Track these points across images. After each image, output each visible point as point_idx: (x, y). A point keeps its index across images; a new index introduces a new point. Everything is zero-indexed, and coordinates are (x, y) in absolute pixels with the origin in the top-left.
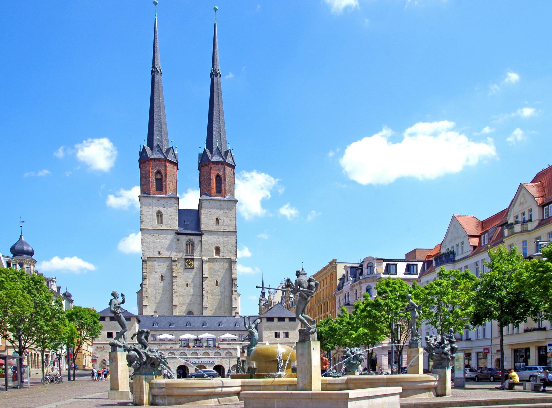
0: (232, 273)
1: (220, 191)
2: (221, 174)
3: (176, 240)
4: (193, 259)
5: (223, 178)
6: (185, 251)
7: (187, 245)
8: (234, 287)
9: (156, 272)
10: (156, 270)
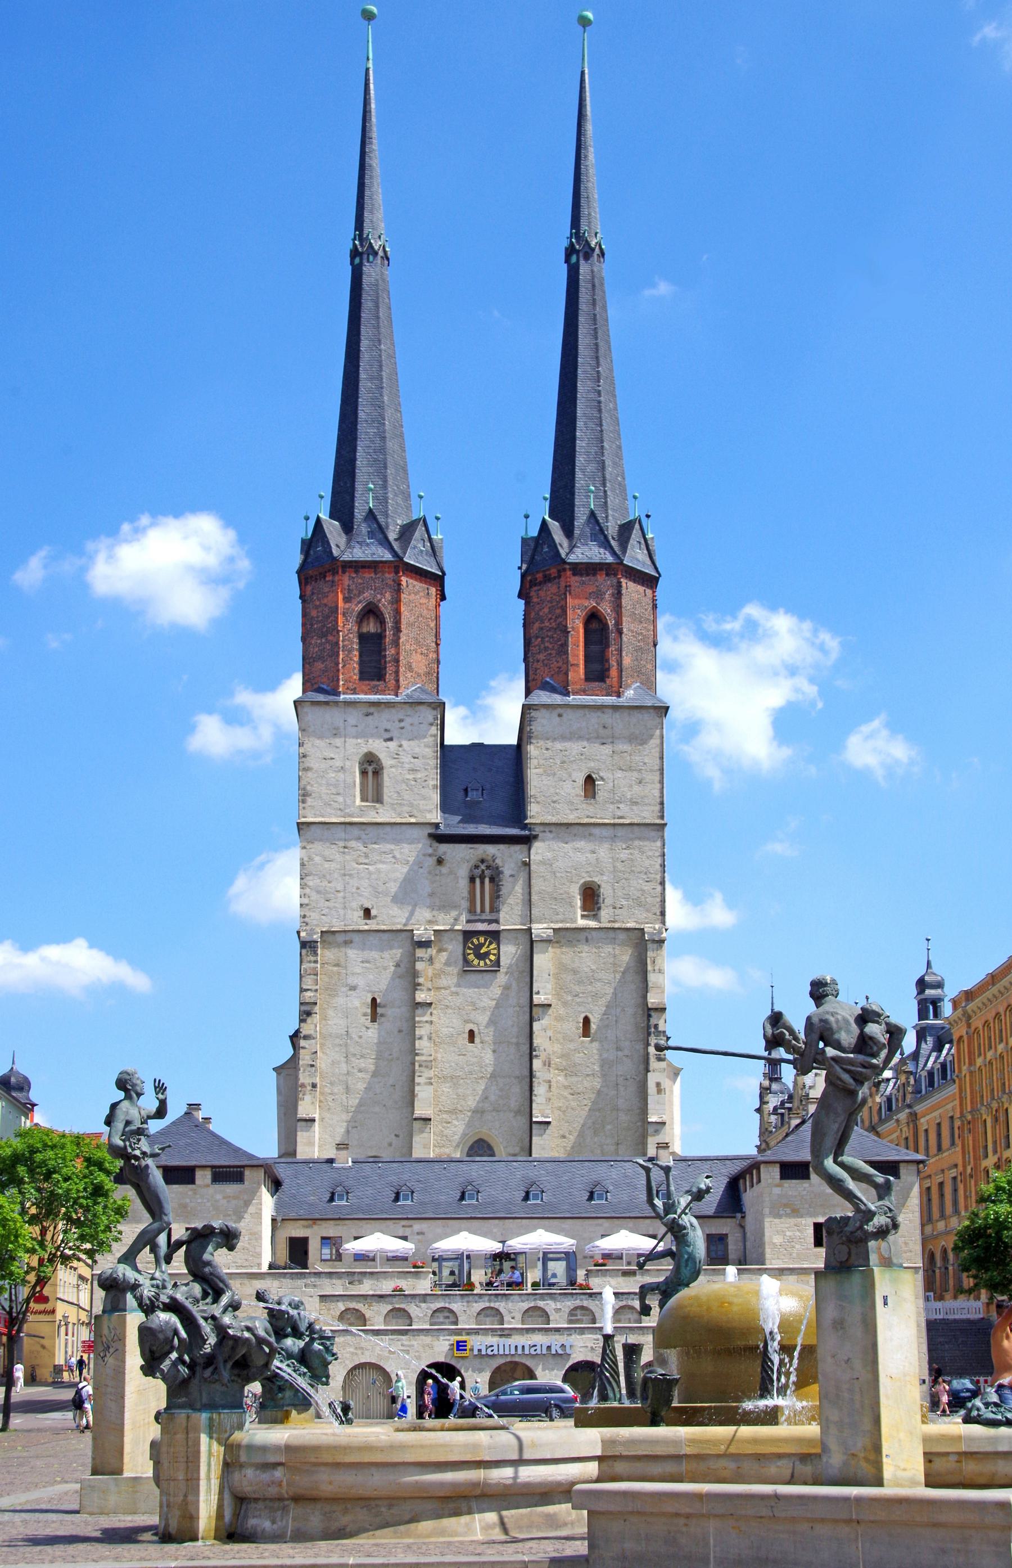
0: (645, 989)
1: (599, 671)
2: (606, 609)
3: (431, 861)
4: (495, 936)
5: (611, 623)
6: (465, 904)
7: (472, 880)
9: (353, 988)
10: (352, 980)
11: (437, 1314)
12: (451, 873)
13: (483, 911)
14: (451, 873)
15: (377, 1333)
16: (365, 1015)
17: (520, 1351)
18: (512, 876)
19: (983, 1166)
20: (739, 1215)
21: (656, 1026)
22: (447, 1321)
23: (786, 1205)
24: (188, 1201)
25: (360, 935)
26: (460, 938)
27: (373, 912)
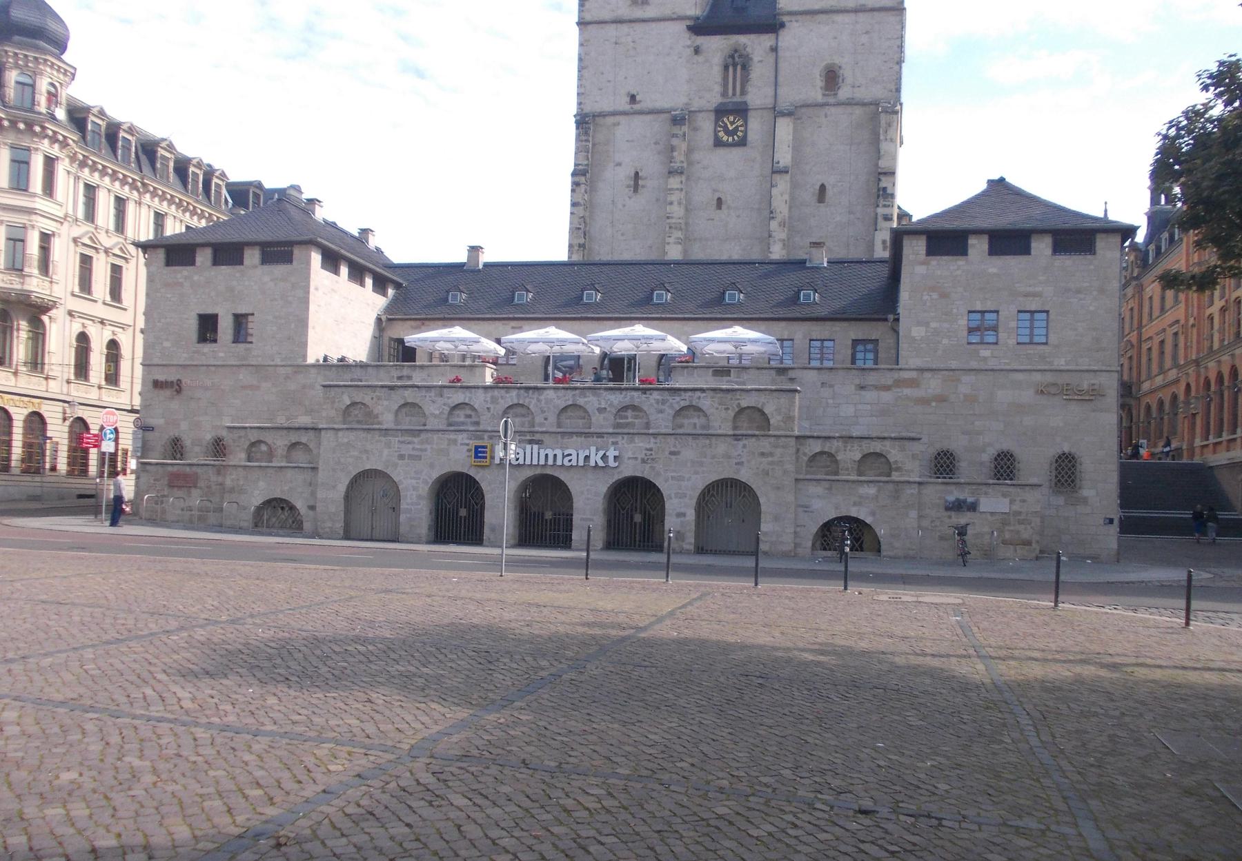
3: (690, 51)
6: (718, 89)
7: (726, 68)
8: (882, 202)
9: (619, 164)
11: (457, 412)
12: (707, 61)
13: (734, 94)
14: (707, 61)
15: (386, 432)
16: (628, 186)
17: (550, 462)
18: (761, 61)
19: (1208, 312)
20: (891, 317)
21: (885, 189)
22: (469, 420)
23: (933, 289)
24: (234, 283)
25: (626, 118)
26: (712, 116)
27: (638, 98)
